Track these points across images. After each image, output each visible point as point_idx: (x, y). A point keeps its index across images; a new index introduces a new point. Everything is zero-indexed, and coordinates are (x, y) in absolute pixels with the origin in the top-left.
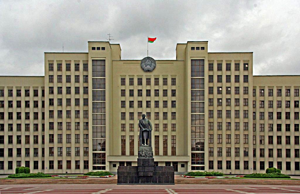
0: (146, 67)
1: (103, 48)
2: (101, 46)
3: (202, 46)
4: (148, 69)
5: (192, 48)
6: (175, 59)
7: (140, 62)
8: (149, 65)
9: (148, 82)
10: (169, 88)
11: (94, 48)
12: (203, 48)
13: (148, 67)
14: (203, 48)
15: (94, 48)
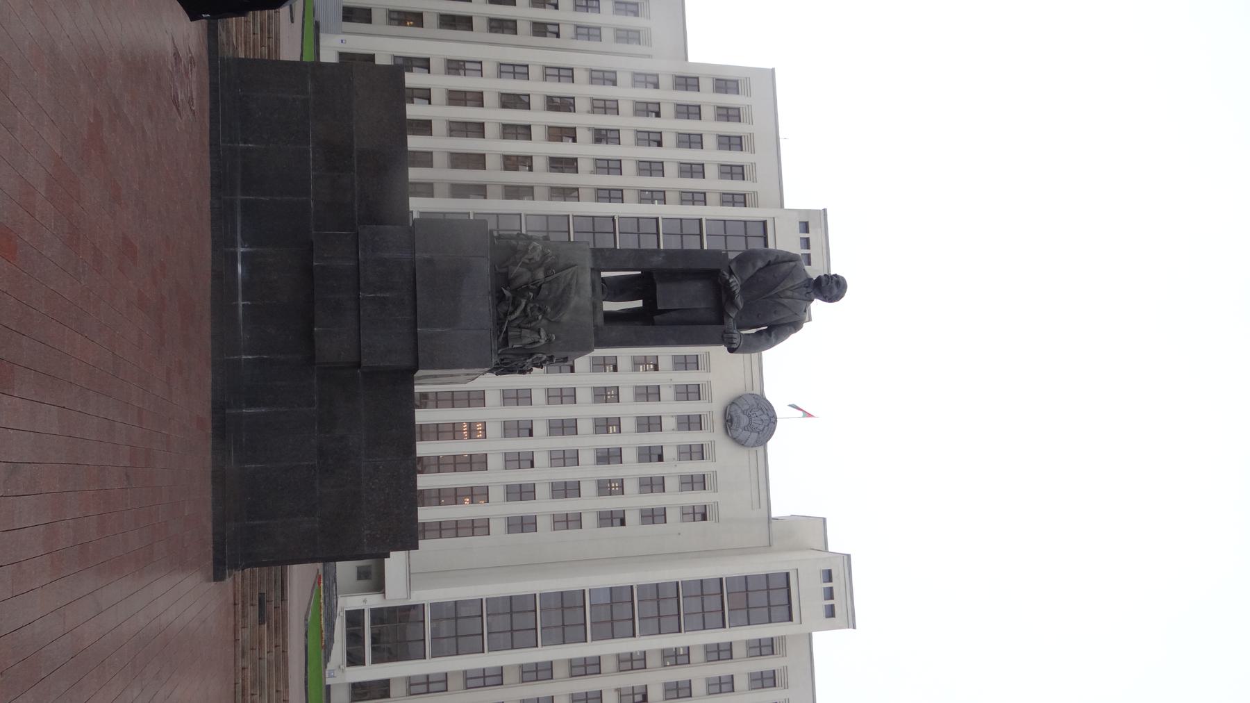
3: (836, 609)
5: (830, 572)
6: (774, 515)
9: (689, 423)
10: (673, 499)
11: (805, 227)
12: (831, 612)
14: (831, 612)
15: (805, 227)
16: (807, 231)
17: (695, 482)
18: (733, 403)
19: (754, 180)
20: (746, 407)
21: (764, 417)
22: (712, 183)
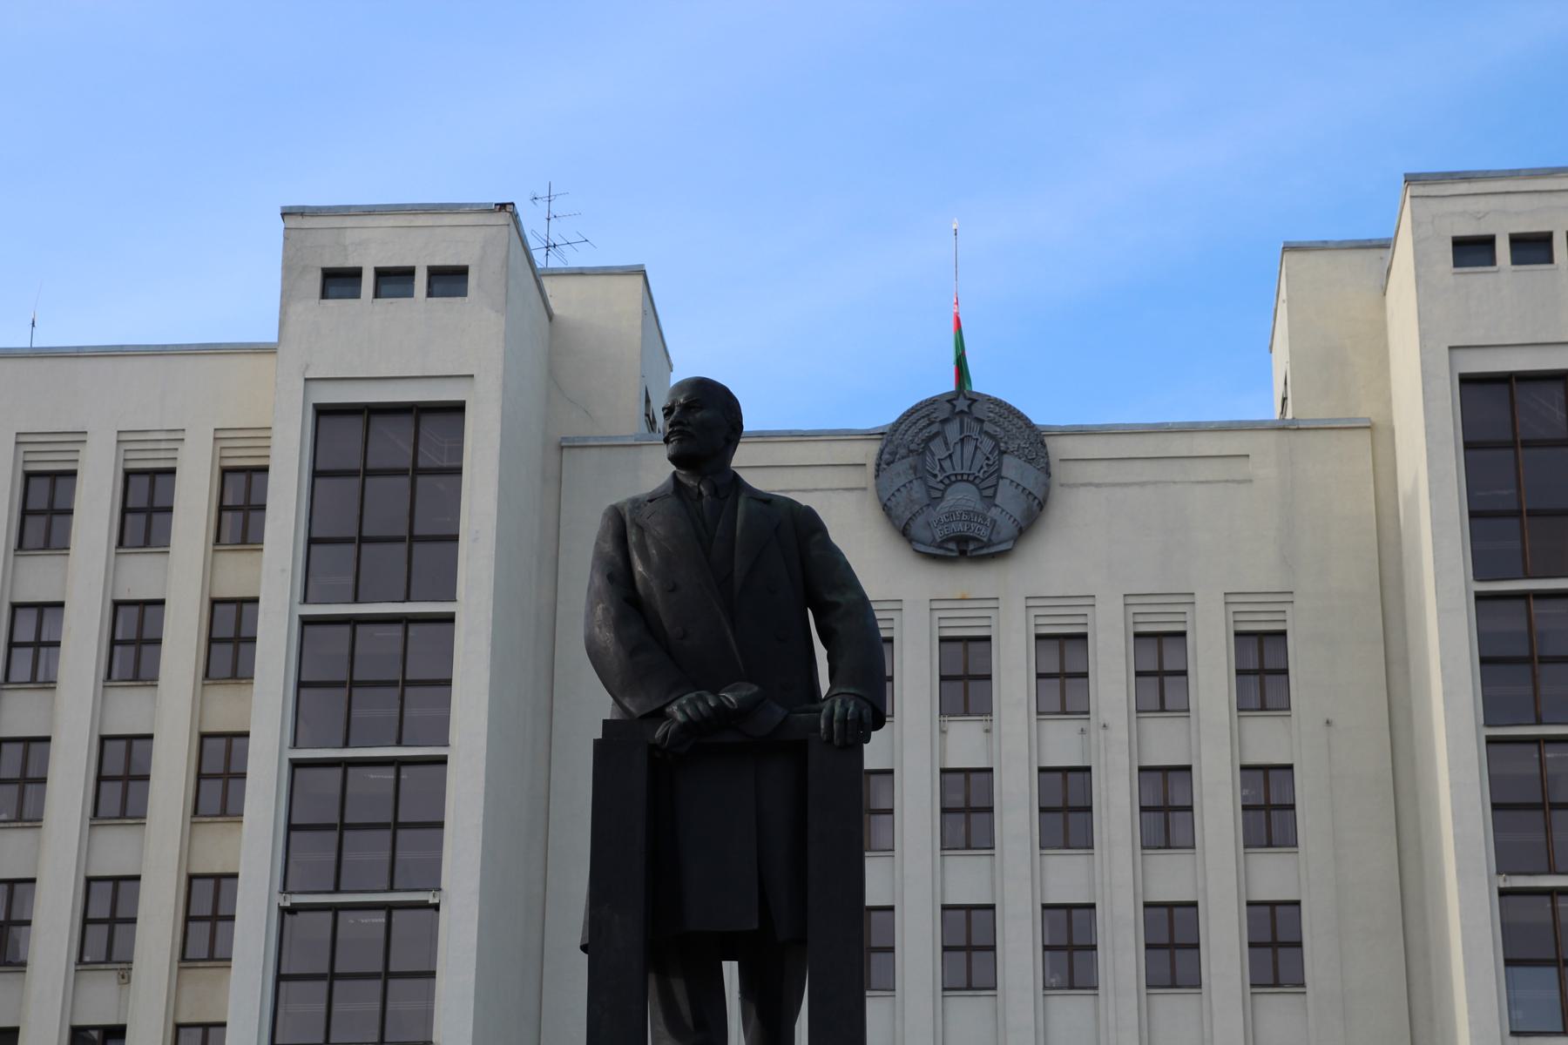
0: (934, 501)
1: (448, 279)
2: (421, 253)
4: (959, 527)
7: (868, 452)
8: (971, 480)
10: (1213, 738)
11: (340, 281)
13: (962, 497)
15: (340, 281)
16: (355, 274)
17: (1161, 665)
18: (905, 533)
19: (176, 437)
20: (918, 491)
21: (953, 431)
22: (182, 575)
